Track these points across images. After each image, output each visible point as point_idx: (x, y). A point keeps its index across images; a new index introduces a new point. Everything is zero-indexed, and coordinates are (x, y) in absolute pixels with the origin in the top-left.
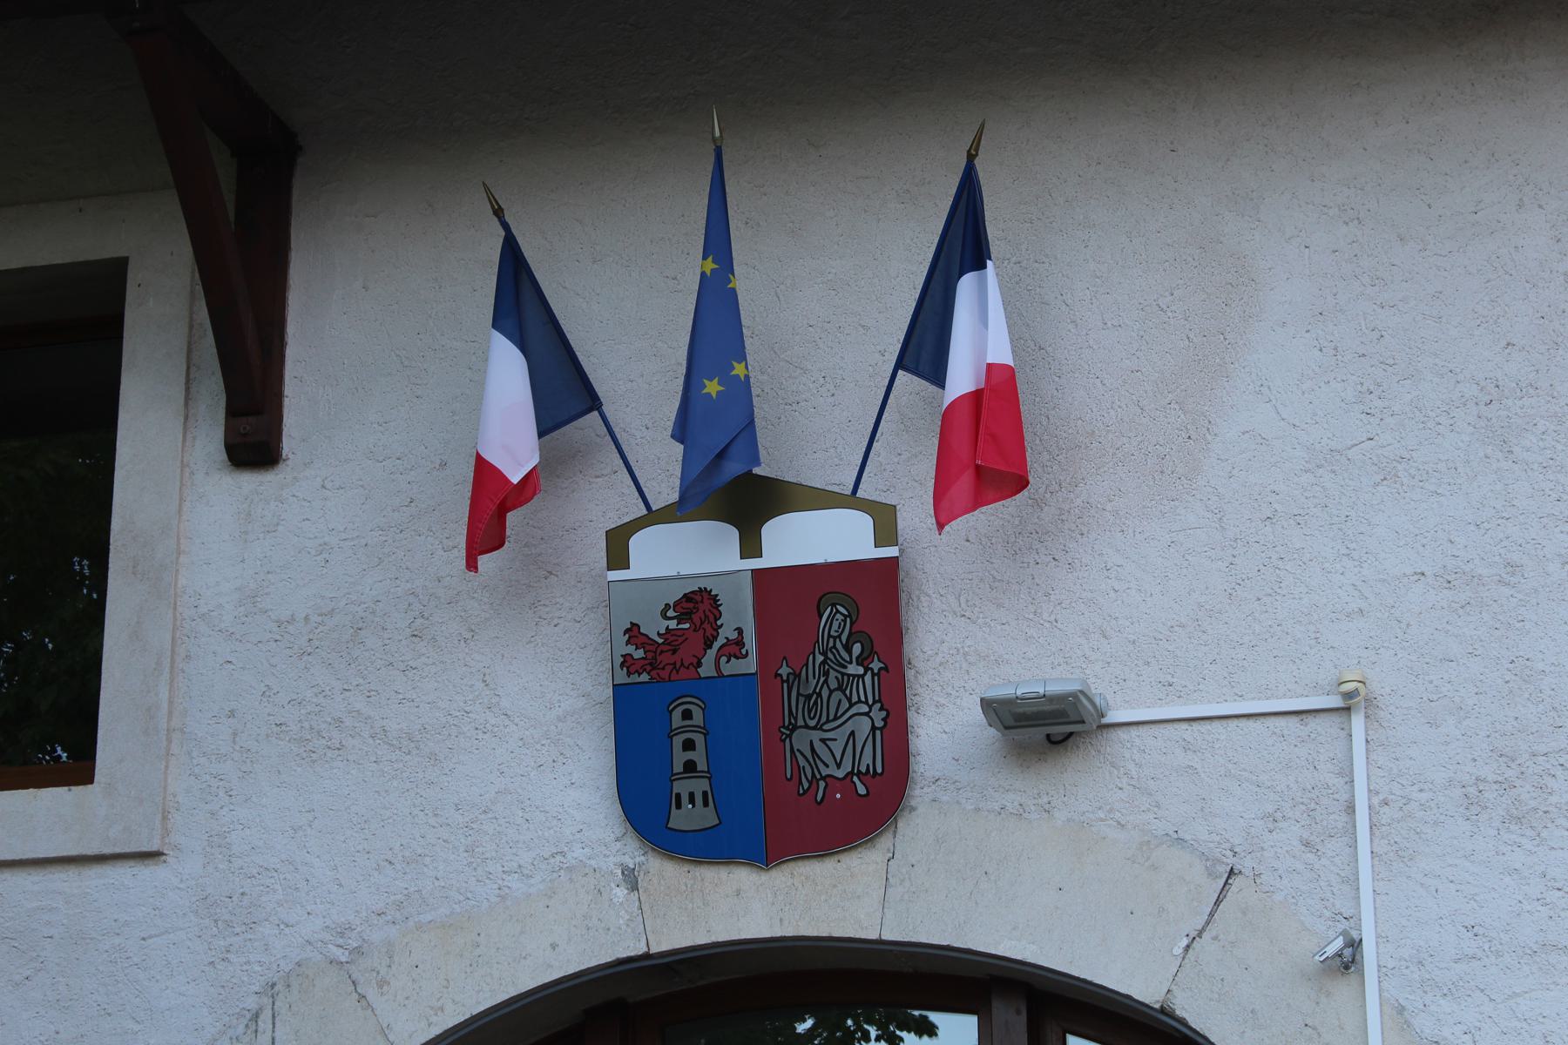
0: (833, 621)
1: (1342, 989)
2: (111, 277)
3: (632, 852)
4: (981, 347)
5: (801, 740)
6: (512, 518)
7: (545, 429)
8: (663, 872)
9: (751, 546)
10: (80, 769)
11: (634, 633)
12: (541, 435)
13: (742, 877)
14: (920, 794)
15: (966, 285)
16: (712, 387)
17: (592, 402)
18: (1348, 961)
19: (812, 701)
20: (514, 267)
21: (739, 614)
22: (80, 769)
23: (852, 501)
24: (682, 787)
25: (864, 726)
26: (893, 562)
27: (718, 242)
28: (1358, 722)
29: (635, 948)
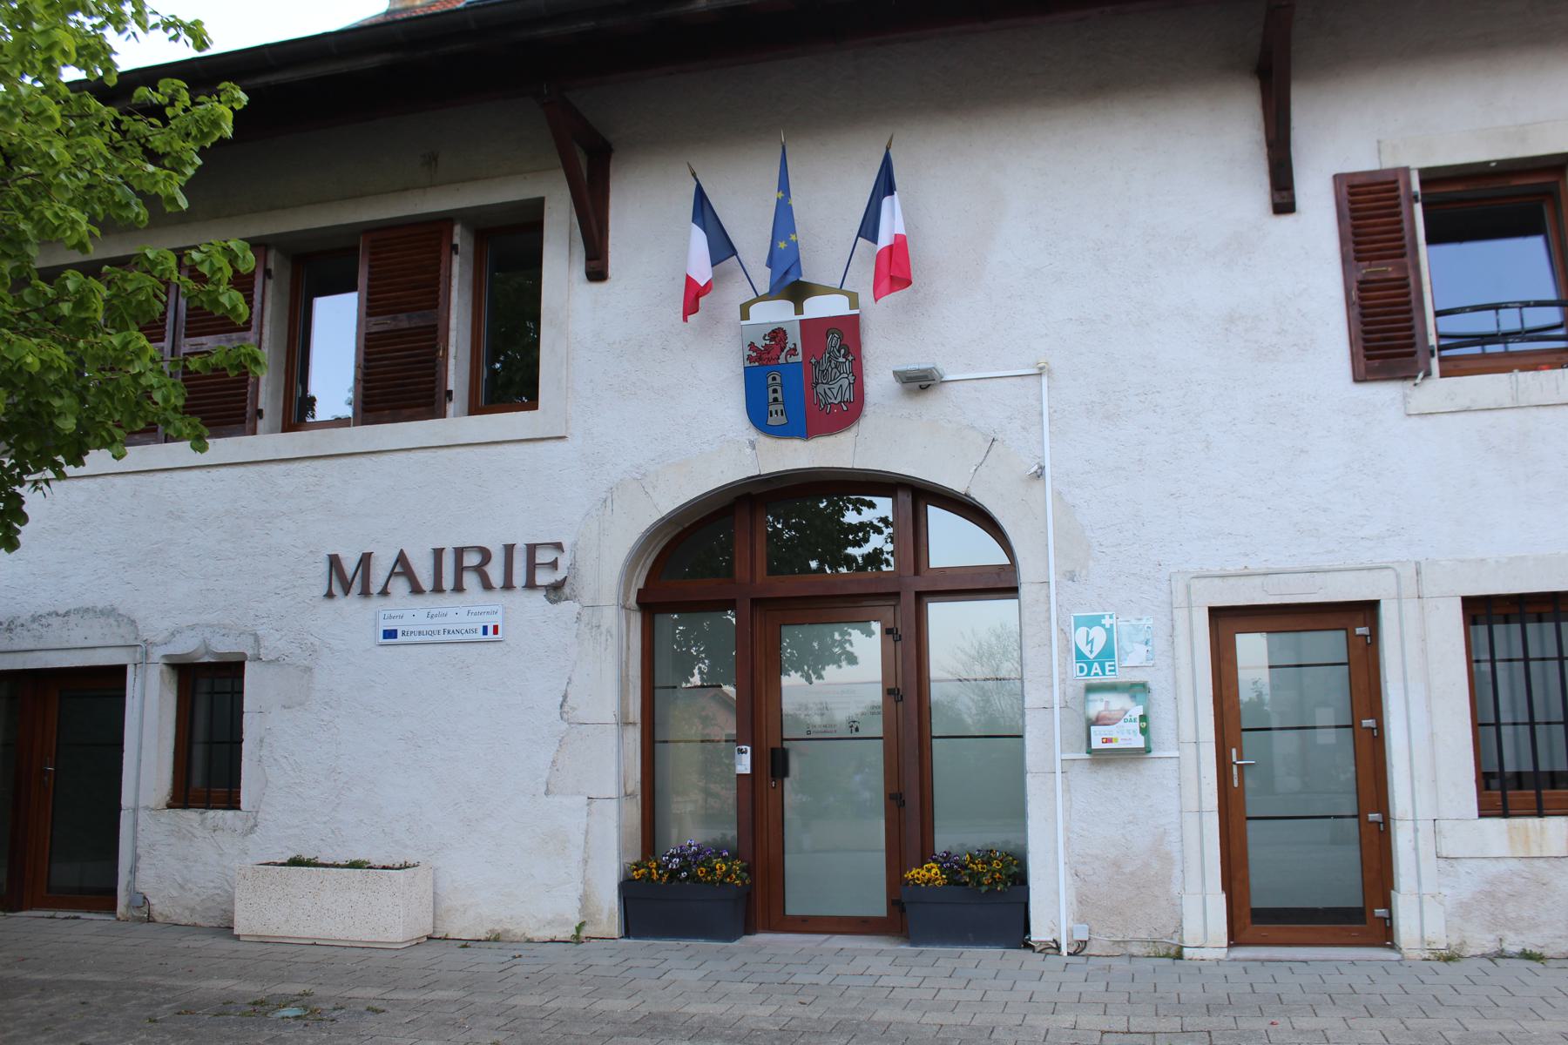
0: (833, 340)
1: (1037, 485)
3: (753, 434)
4: (892, 227)
5: (820, 388)
6: (702, 300)
7: (715, 262)
9: (799, 310)
10: (532, 402)
11: (752, 346)
12: (713, 266)
13: (797, 444)
14: (868, 409)
15: (886, 201)
16: (782, 245)
17: (734, 252)
18: (1039, 475)
19: (824, 373)
20: (701, 198)
21: (794, 338)
22: (532, 402)
23: (840, 291)
24: (772, 408)
25: (845, 383)
26: (856, 317)
27: (784, 185)
28: (1045, 380)
29: (755, 472)
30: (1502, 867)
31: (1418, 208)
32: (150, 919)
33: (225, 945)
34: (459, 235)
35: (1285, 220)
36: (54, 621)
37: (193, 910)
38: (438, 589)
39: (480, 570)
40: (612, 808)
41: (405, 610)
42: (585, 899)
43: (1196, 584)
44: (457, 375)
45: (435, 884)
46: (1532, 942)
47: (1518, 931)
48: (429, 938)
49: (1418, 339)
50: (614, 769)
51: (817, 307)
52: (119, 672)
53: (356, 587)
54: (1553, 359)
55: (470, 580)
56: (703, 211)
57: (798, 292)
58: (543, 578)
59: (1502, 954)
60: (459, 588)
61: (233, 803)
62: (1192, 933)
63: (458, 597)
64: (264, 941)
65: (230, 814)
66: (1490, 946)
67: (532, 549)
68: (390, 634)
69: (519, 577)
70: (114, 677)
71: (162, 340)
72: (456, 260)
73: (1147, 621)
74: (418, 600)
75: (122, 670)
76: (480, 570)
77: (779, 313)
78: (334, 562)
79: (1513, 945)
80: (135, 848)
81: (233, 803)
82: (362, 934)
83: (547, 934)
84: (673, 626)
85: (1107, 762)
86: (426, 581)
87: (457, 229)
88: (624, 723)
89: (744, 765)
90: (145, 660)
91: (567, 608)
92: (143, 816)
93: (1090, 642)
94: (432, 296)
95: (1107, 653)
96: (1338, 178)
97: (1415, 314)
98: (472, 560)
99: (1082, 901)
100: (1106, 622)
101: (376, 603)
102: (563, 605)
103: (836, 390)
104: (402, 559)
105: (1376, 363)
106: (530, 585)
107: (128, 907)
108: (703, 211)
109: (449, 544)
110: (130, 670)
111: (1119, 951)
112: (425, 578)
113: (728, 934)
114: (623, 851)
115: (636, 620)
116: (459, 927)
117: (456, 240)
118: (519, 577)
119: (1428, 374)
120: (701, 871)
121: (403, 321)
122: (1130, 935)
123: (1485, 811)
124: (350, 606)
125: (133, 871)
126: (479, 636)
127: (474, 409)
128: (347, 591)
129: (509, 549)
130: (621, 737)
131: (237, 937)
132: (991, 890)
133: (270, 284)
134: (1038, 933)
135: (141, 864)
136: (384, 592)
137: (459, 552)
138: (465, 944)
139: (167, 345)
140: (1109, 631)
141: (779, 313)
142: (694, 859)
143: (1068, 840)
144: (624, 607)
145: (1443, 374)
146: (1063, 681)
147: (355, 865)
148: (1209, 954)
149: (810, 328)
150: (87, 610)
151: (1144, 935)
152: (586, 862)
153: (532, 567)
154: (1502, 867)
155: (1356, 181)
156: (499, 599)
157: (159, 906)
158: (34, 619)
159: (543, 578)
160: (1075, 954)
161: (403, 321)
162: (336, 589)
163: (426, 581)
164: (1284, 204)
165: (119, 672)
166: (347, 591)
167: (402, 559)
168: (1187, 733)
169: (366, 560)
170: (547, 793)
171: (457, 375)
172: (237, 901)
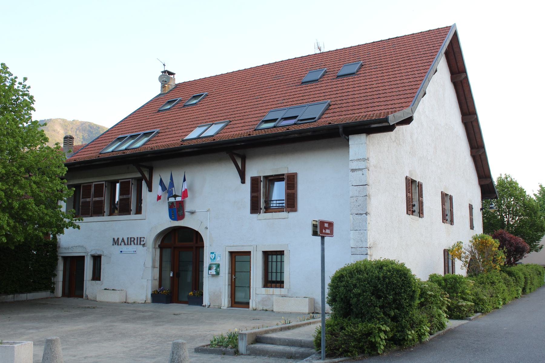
4: (185, 187)
5: (179, 212)
8: (172, 221)
9: (175, 199)
13: (176, 222)
18: (206, 228)
21: (175, 204)
32: (88, 299)
35: (244, 185)
36: (75, 248)
38: (128, 244)
40: (150, 281)
41: (123, 248)
42: (146, 296)
44: (133, 207)
45: (126, 293)
46: (267, 308)
47: (266, 306)
48: (125, 302)
49: (259, 207)
50: (150, 275)
51: (179, 199)
52: (83, 257)
53: (117, 244)
55: (132, 243)
58: (142, 243)
60: (131, 244)
61: (100, 280)
62: (223, 305)
64: (101, 302)
65: (99, 281)
67: (140, 238)
68: (121, 252)
69: (139, 243)
70: (83, 257)
71: (90, 198)
75: (84, 257)
76: (133, 241)
77: (172, 200)
78: (114, 239)
81: (100, 280)
82: (113, 301)
83: (141, 302)
87: (133, 180)
88: (154, 267)
89: (171, 275)
91: (145, 248)
92: (87, 281)
93: (212, 256)
95: (215, 258)
96: (251, 177)
98: (132, 239)
99: (210, 299)
100: (215, 253)
101: (120, 246)
102: (145, 247)
103: (180, 213)
104: (123, 239)
106: (140, 244)
107: (85, 297)
109: (130, 237)
110: (85, 257)
111: (214, 307)
114: (152, 288)
115: (158, 251)
116: (130, 301)
118: (139, 243)
119: (260, 213)
121: (125, 197)
124: (116, 246)
125: (86, 291)
126: (133, 252)
128: (115, 244)
129: (137, 238)
130: (153, 271)
131: (97, 301)
134: (204, 304)
137: (131, 238)
139: (91, 199)
140: (215, 255)
141: (172, 200)
145: (265, 212)
146: (209, 263)
147: (113, 290)
149: (178, 202)
151: (217, 305)
152: (147, 290)
153: (140, 241)
155: (254, 178)
156: (136, 246)
157: (89, 297)
158: (72, 247)
159: (142, 243)
160: (208, 307)
162: (114, 244)
164: (243, 181)
165: (83, 257)
167: (123, 239)
168: (224, 272)
169: (118, 239)
170: (142, 279)
172: (97, 296)
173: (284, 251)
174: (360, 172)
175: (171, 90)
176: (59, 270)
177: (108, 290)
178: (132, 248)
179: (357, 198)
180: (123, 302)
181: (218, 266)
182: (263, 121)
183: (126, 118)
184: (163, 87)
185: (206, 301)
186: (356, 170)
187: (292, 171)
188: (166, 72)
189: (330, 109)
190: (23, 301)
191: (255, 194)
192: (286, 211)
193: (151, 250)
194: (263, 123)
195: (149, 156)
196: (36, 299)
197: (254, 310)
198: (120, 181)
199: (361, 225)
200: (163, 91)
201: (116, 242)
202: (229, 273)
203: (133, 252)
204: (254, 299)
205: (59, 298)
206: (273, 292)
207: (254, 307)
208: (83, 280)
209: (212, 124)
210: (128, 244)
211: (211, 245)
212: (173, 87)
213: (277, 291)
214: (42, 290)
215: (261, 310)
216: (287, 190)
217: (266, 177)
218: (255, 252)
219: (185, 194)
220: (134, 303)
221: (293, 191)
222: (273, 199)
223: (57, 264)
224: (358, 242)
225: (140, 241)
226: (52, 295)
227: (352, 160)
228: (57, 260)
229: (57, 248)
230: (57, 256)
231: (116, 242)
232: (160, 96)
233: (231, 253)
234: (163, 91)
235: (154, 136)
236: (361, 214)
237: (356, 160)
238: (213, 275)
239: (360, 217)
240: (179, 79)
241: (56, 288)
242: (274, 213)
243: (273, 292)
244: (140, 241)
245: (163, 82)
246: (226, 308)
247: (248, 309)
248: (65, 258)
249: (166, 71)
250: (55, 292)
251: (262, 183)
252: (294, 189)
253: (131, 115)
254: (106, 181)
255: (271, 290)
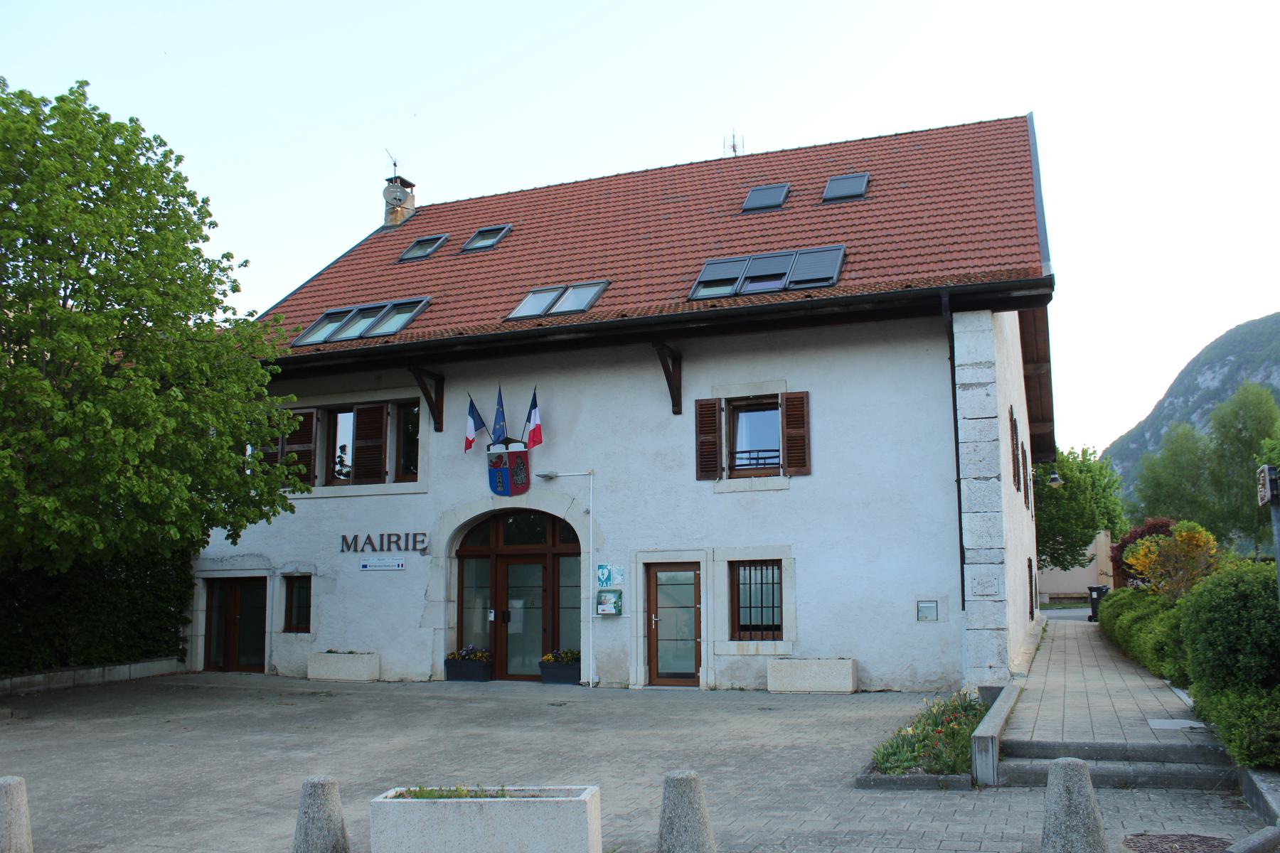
0: (519, 460)
2: (419, 398)
3: (492, 494)
9: (507, 449)
10: (415, 480)
13: (507, 498)
15: (533, 411)
18: (588, 512)
19: (516, 472)
20: (472, 405)
21: (505, 459)
22: (415, 480)
27: (500, 403)
30: (735, 658)
31: (723, 414)
32: (277, 675)
33: (304, 682)
34: (390, 408)
35: (678, 417)
36: (239, 559)
37: (293, 671)
38: (382, 549)
39: (396, 542)
40: (442, 633)
41: (371, 558)
42: (433, 666)
43: (639, 555)
44: (390, 465)
45: (380, 661)
46: (743, 685)
48: (378, 681)
50: (443, 619)
51: (516, 447)
52: (264, 579)
53: (352, 548)
54: (771, 471)
55: (393, 546)
56: (473, 411)
57: (507, 442)
58: (419, 546)
59: (733, 689)
60: (389, 549)
61: (307, 630)
62: (632, 680)
63: (389, 553)
64: (318, 680)
65: (306, 634)
66: (729, 686)
67: (415, 535)
68: (365, 566)
69: (411, 546)
70: (262, 581)
72: (389, 418)
73: (622, 568)
74: (375, 554)
75: (265, 578)
76: (396, 542)
77: (499, 449)
78: (344, 538)
79: (737, 685)
80: (271, 647)
81: (307, 630)
83: (419, 679)
84: (471, 564)
85: (607, 618)
86: (377, 546)
87: (389, 405)
88: (448, 600)
89: (492, 617)
90: (273, 575)
92: (274, 635)
93: (603, 575)
94: (380, 433)
95: (609, 578)
96: (697, 401)
97: (718, 455)
98: (394, 539)
99: (598, 668)
100: (609, 567)
101: (359, 554)
103: (520, 479)
104: (369, 538)
105: (704, 473)
106: (415, 549)
108: (473, 411)
109: (386, 532)
110: (268, 578)
112: (377, 545)
113: (485, 680)
114: (446, 648)
115: (455, 563)
116: (388, 677)
117: (389, 410)
118: (411, 546)
119: (721, 478)
120: (472, 656)
121: (370, 443)
122: (613, 681)
123: (732, 638)
124: (350, 555)
125: (271, 656)
126: (397, 568)
127: (398, 479)
128: (349, 549)
129: (407, 535)
130: (446, 608)
131: (309, 680)
132: (567, 663)
133: (319, 423)
134: (583, 680)
135: (274, 654)
136: (363, 550)
137: (389, 536)
138: (389, 682)
139: (279, 447)
141: (499, 449)
142: (474, 651)
143: (593, 646)
144: (449, 557)
145: (730, 477)
146: (593, 589)
147: (351, 653)
148: (636, 687)
149: (511, 454)
150: (251, 555)
151: (618, 681)
152: (433, 652)
153: (415, 542)
154: (735, 658)
155: (703, 403)
156: (403, 554)
157: (280, 670)
158: (231, 557)
159: (419, 546)
161: (370, 443)
162: (345, 549)
163: (377, 546)
164: (677, 409)
165: (264, 579)
166: (349, 549)
167: (369, 538)
168: (634, 609)
169: (356, 538)
170: (420, 627)
171: (390, 465)
172: (309, 667)
173: (781, 560)
174: (982, 391)
175: (407, 220)
176: (197, 610)
177: (334, 652)
178: (392, 558)
179: (977, 444)
180: (373, 681)
181: (619, 594)
182: (700, 283)
183: (320, 274)
184: (391, 210)
185: (588, 671)
186: (971, 385)
187: (795, 387)
188: (398, 181)
189: (850, 262)
190: (121, 681)
191: (709, 438)
192: (785, 475)
193: (443, 561)
194: (700, 287)
195: (459, 348)
196: (149, 677)
197: (714, 689)
198: (355, 408)
199: (986, 502)
200: (391, 220)
201: (349, 545)
202: (644, 612)
203: (397, 568)
204: (711, 665)
205: (199, 672)
206: (757, 649)
207: (712, 682)
208: (264, 632)
209: (566, 289)
210: (382, 549)
211: (598, 550)
212: (412, 213)
213: (766, 646)
214: (161, 656)
215: (727, 690)
216: (787, 428)
217: (729, 401)
218: (710, 564)
219: (536, 437)
220: (401, 681)
221: (801, 431)
222: (738, 450)
223: (192, 595)
224: (981, 537)
225: (415, 543)
226: (181, 668)
227: (962, 365)
228: (191, 586)
229: (190, 560)
230: (192, 577)
231: (349, 545)
232: (384, 232)
233: (648, 566)
234: (391, 220)
235: (422, 311)
236: (987, 479)
237: (971, 365)
238: (606, 616)
239: (983, 484)
240: (423, 197)
241: (189, 652)
242: (753, 479)
243: (757, 649)
244: (415, 543)
245: (394, 202)
246: (641, 687)
247: (696, 689)
248: (210, 582)
249: (399, 177)
250: (187, 659)
251: (723, 414)
252: (803, 427)
253: (328, 268)
254: (318, 408)
255: (751, 646)
